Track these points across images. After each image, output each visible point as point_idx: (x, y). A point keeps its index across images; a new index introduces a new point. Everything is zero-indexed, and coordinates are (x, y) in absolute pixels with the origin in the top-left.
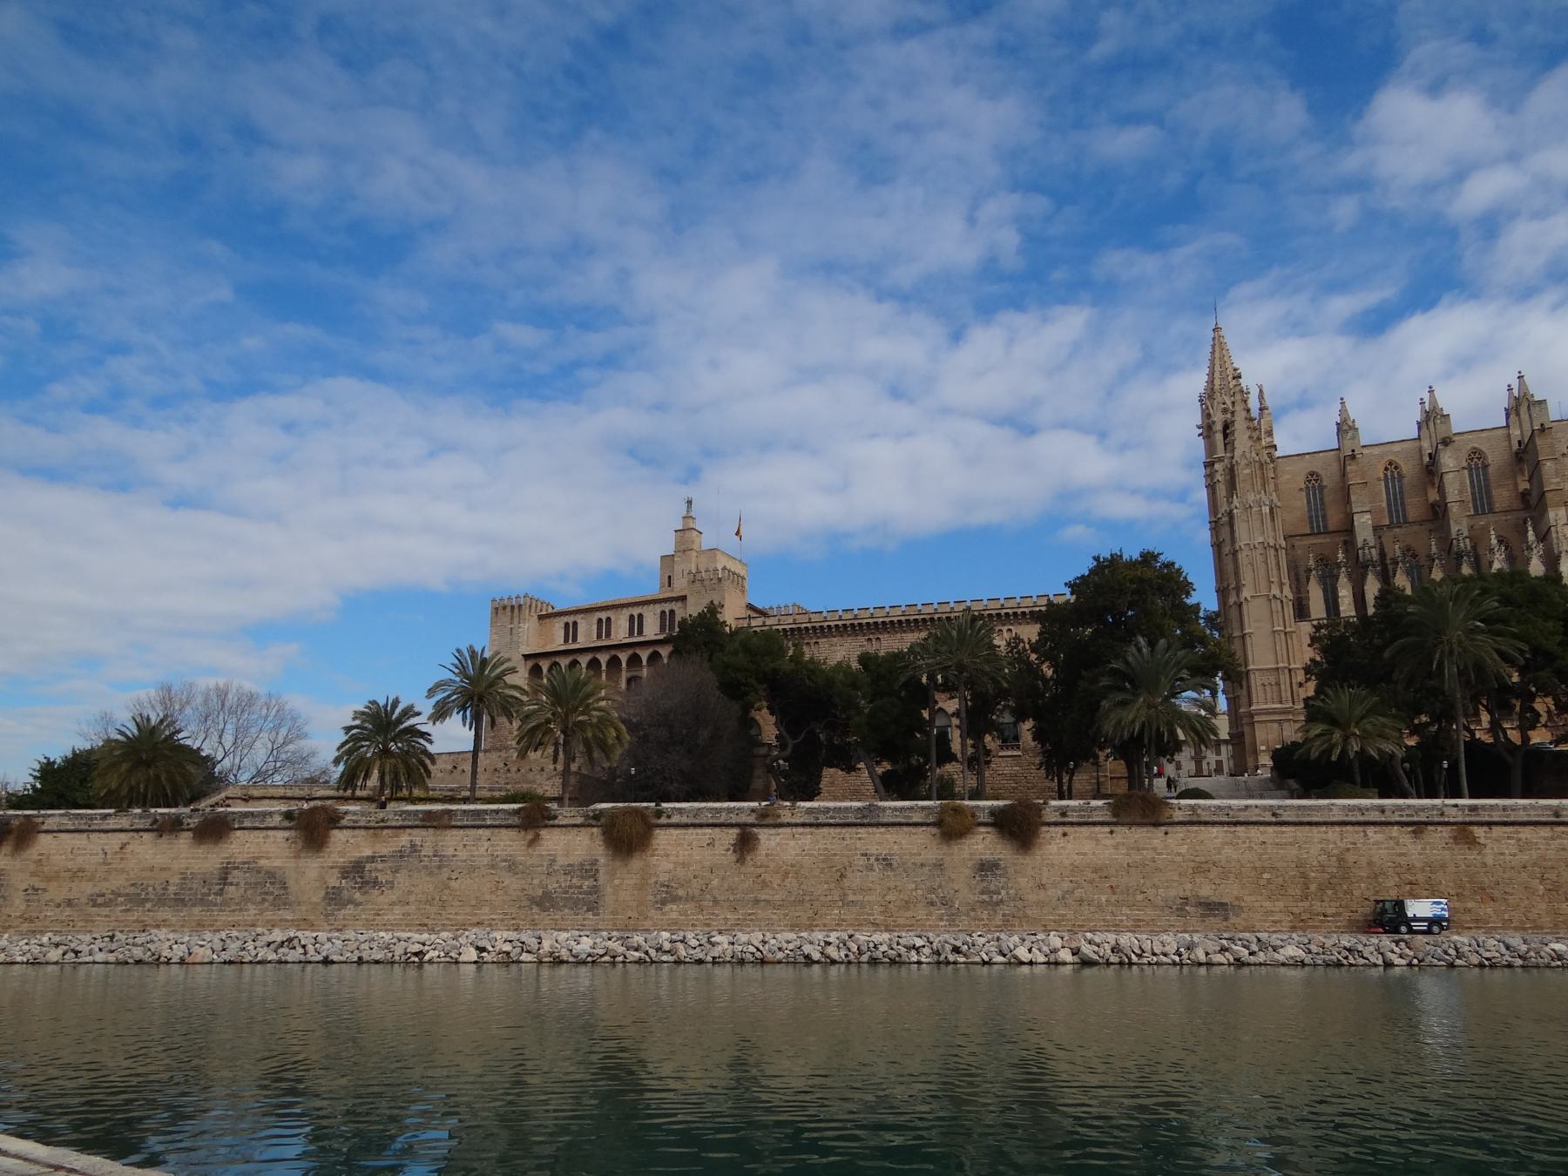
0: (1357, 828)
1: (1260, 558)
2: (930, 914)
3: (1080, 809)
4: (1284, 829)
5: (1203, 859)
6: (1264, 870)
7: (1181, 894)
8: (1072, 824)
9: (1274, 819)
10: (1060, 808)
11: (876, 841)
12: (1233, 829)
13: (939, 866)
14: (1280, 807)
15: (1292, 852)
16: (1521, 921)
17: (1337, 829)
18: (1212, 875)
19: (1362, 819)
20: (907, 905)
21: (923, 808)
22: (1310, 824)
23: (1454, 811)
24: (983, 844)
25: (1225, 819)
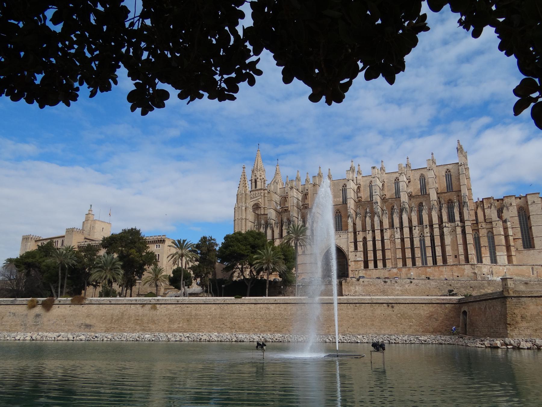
0: (129, 305)
1: (240, 222)
2: (20, 328)
3: (64, 300)
4: (112, 305)
5: (90, 313)
6: (103, 316)
7: (82, 323)
8: (61, 304)
9: (109, 303)
10: (59, 300)
11: (13, 309)
12: (99, 305)
13: (26, 315)
14: (112, 300)
15: (112, 311)
16: (161, 330)
17: (124, 305)
18: (90, 318)
19: (130, 303)
20: (16, 325)
21: (27, 300)
22: (118, 304)
23: (153, 301)
24: (38, 309)
25: (98, 303)
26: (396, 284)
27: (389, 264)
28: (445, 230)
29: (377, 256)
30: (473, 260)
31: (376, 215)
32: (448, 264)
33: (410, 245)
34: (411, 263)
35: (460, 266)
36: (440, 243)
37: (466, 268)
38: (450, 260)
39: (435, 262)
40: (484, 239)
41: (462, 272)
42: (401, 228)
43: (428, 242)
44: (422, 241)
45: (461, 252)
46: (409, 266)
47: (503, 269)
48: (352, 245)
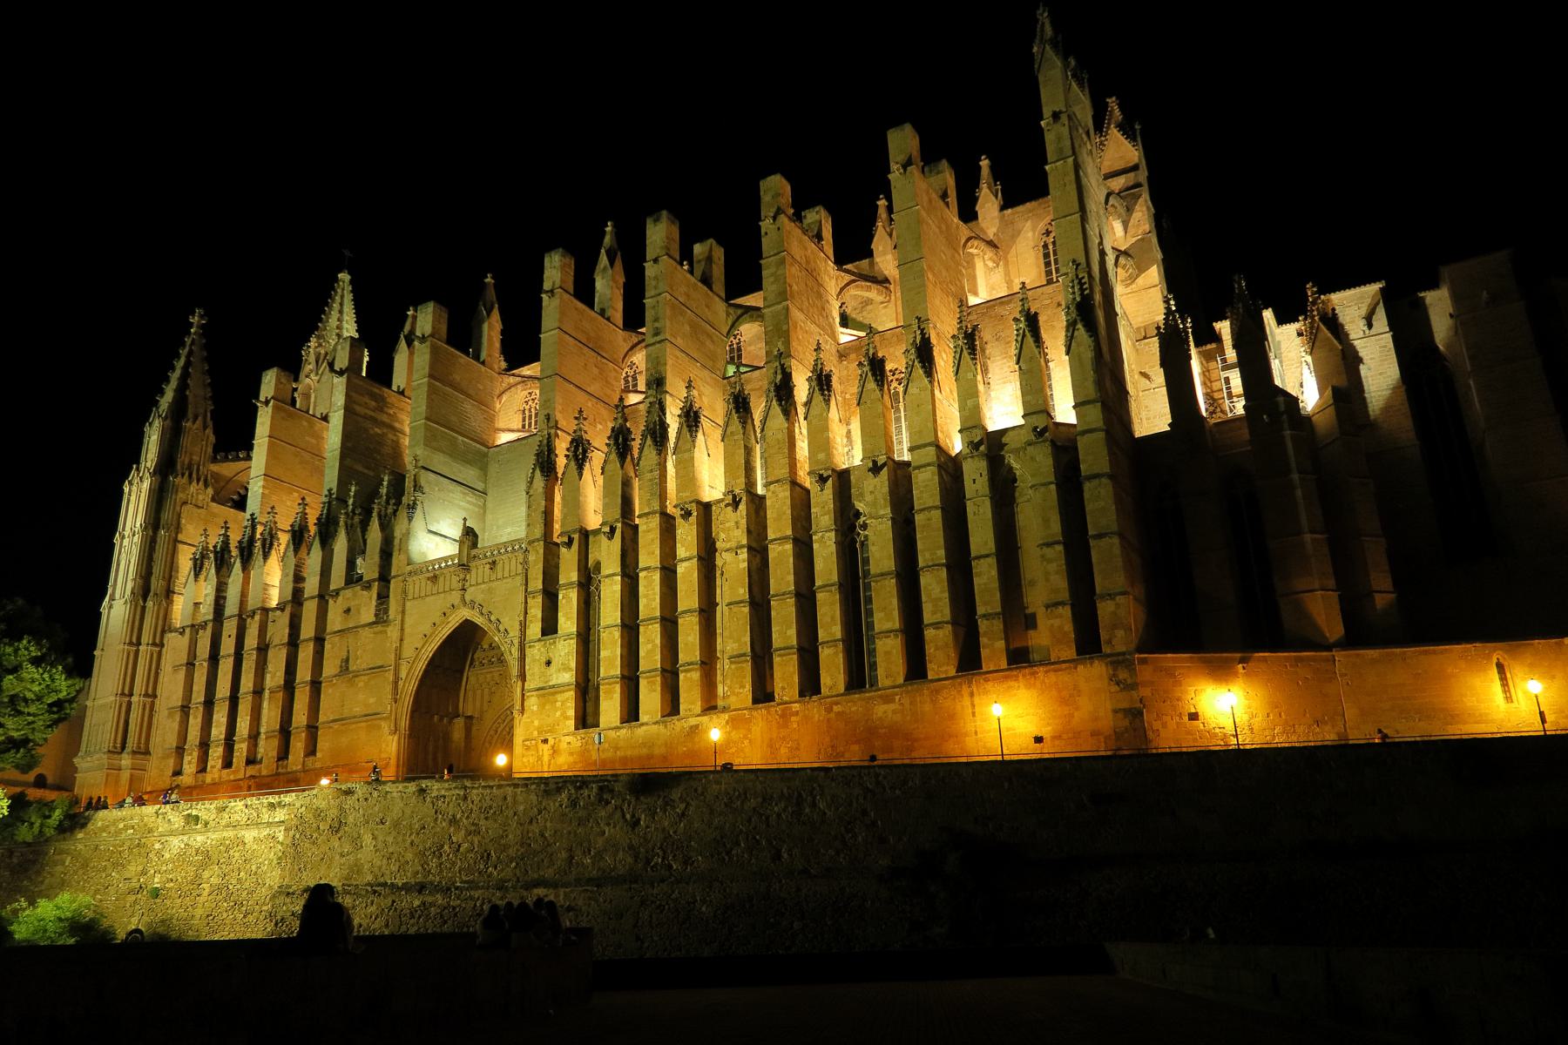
29: (642, 653)
33: (791, 578)
36: (941, 553)
38: (993, 648)
39: (916, 668)
48: (536, 611)
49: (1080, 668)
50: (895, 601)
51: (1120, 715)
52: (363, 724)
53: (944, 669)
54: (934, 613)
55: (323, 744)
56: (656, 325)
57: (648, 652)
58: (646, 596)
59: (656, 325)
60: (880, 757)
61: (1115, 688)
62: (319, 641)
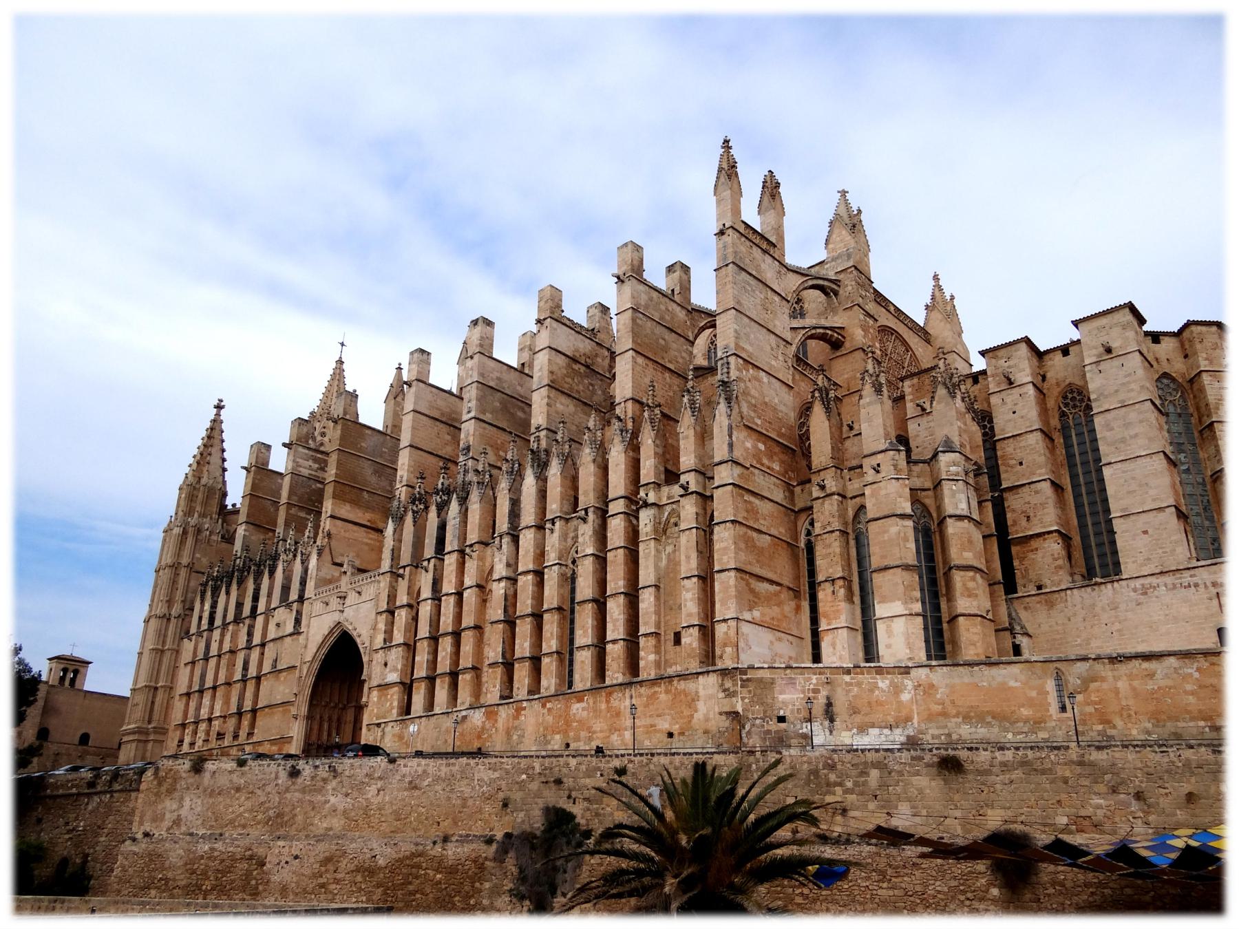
26: (334, 783)
27: (465, 695)
28: (645, 516)
29: (439, 659)
30: (729, 650)
31: (455, 496)
32: (640, 679)
33: (529, 602)
34: (527, 681)
35: (682, 685)
37: (702, 693)
38: (647, 658)
40: (830, 546)
41: (686, 713)
42: (515, 540)
43: (585, 588)
44: (570, 580)
45: (690, 615)
46: (520, 698)
47: (897, 690)
49: (701, 677)
50: (590, 621)
51: (724, 717)
52: (281, 709)
53: (616, 675)
54: (613, 631)
55: (259, 723)
56: (470, 405)
57: (443, 658)
58: (445, 615)
59: (470, 405)
60: (573, 746)
61: (721, 695)
62: (263, 645)
